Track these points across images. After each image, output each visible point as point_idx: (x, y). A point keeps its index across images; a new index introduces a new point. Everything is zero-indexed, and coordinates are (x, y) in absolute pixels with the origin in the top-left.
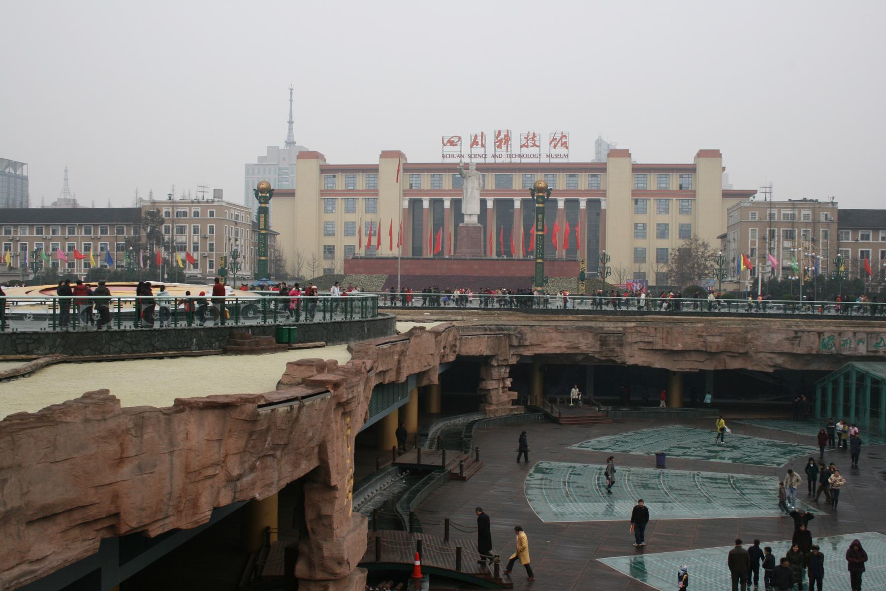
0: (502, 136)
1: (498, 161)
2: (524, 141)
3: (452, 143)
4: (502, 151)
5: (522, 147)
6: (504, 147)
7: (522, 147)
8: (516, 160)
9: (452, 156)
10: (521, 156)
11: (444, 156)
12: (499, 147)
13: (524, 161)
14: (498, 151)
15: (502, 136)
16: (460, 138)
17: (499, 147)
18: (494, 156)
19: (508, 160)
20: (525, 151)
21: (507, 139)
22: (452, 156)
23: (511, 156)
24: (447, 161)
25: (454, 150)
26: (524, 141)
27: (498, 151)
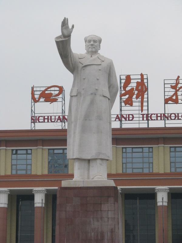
0: (133, 85)
1: (127, 125)
2: (171, 92)
3: (48, 97)
4: (134, 109)
5: (166, 101)
6: (136, 103)
7: (166, 101)
8: (160, 124)
9: (49, 119)
10: (165, 117)
11: (34, 120)
12: (129, 102)
13: (171, 124)
14: (127, 110)
15: (133, 85)
16: (61, 90)
17: (129, 102)
18: (120, 118)
19: (144, 125)
20: (172, 108)
21: (142, 88)
22: (49, 119)
23: (148, 117)
24: (39, 126)
25: (53, 109)
26: (171, 92)
27: (127, 110)
